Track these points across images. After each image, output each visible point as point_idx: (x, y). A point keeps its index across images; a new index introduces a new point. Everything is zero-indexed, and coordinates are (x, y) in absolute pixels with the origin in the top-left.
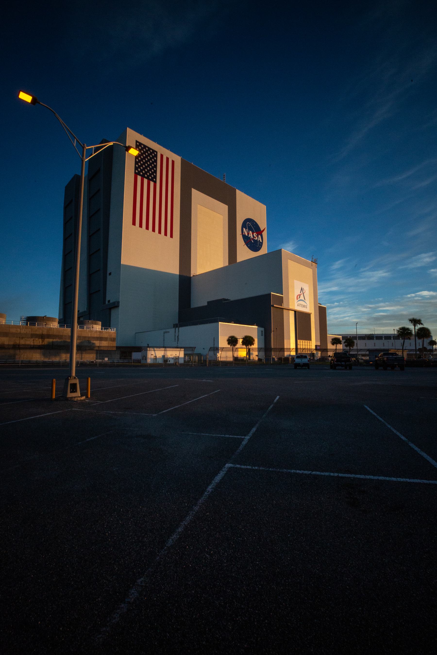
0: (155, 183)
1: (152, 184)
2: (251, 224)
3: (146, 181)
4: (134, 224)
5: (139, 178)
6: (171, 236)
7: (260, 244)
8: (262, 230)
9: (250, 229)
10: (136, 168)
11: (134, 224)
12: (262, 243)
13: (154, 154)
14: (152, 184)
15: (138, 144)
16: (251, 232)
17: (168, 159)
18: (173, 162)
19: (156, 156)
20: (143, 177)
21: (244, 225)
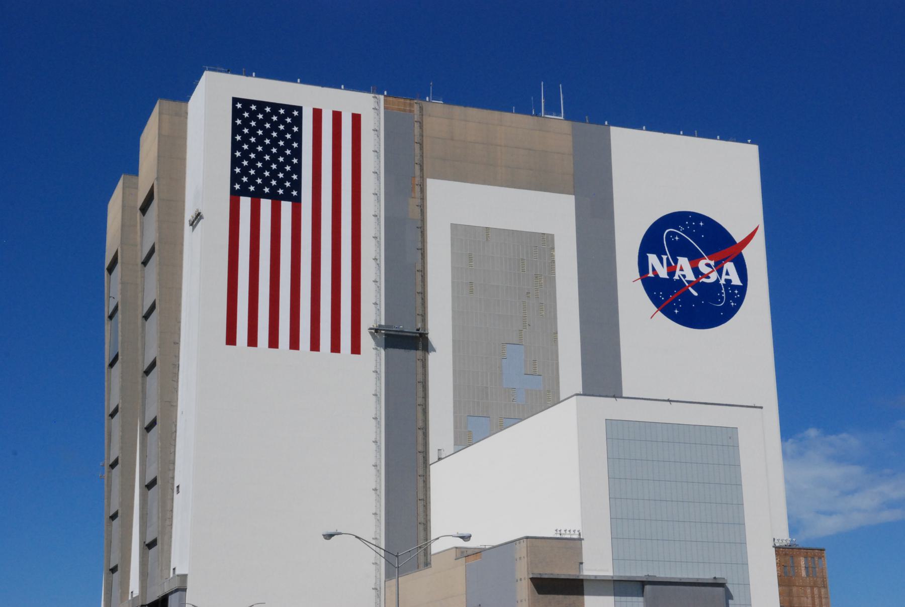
0: (297, 202)
1: (286, 207)
2: (686, 233)
3: (266, 205)
4: (231, 339)
5: (245, 203)
6: (356, 348)
7: (730, 296)
8: (738, 238)
9: (679, 249)
10: (235, 178)
11: (231, 339)
12: (743, 290)
13: (292, 116)
14: (286, 207)
15: (239, 106)
16: (683, 262)
17: (337, 117)
18: (356, 119)
19: (298, 121)
20: (256, 197)
21: (652, 242)
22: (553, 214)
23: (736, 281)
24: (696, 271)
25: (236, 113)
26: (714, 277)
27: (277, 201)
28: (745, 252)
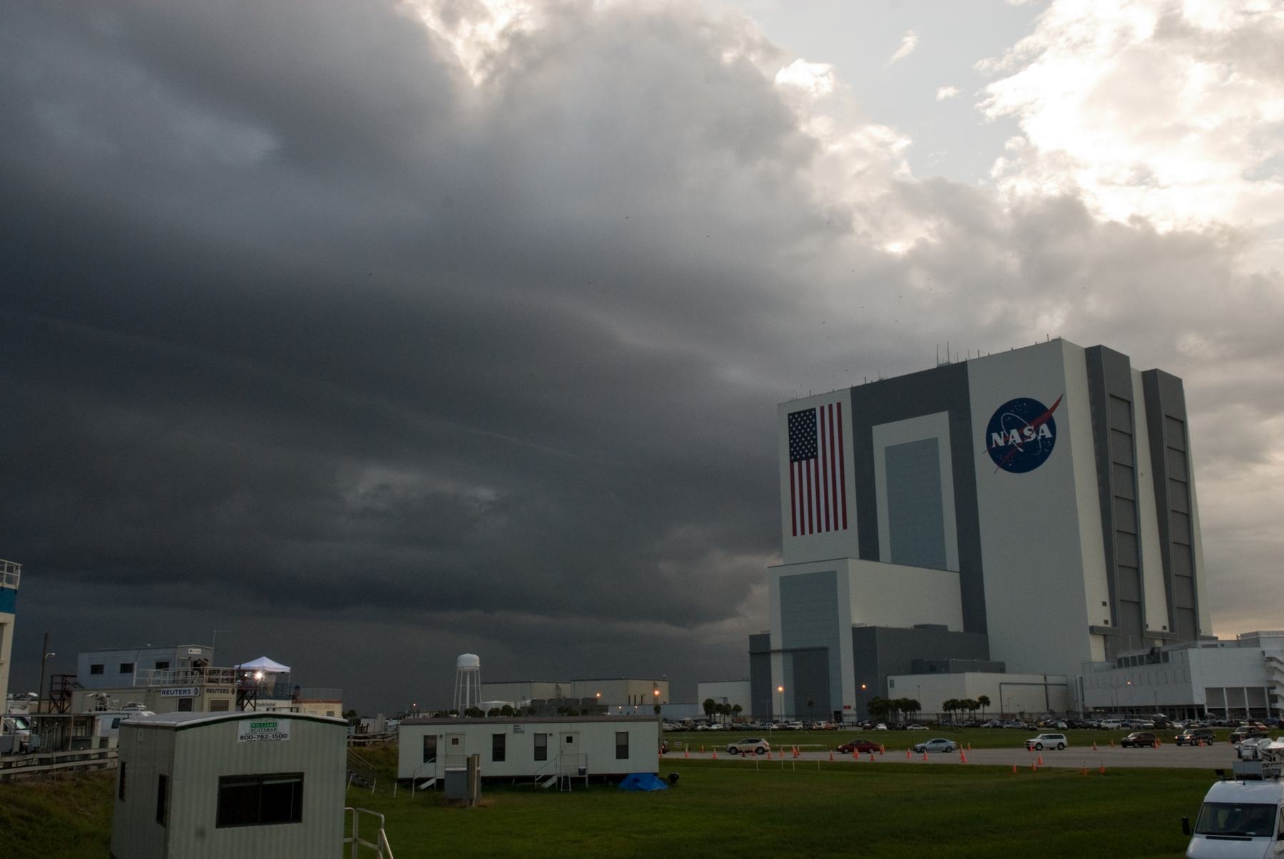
0: (816, 457)
1: (812, 461)
3: (804, 463)
4: (795, 534)
5: (796, 464)
6: (845, 527)
8: (1049, 407)
10: (791, 454)
11: (795, 534)
12: (1053, 440)
14: (812, 461)
16: (1014, 432)
18: (839, 405)
19: (814, 416)
21: (994, 426)
22: (936, 426)
23: (1048, 435)
24: (1022, 436)
25: (790, 421)
26: (1034, 436)
27: (808, 459)
28: (1055, 415)
